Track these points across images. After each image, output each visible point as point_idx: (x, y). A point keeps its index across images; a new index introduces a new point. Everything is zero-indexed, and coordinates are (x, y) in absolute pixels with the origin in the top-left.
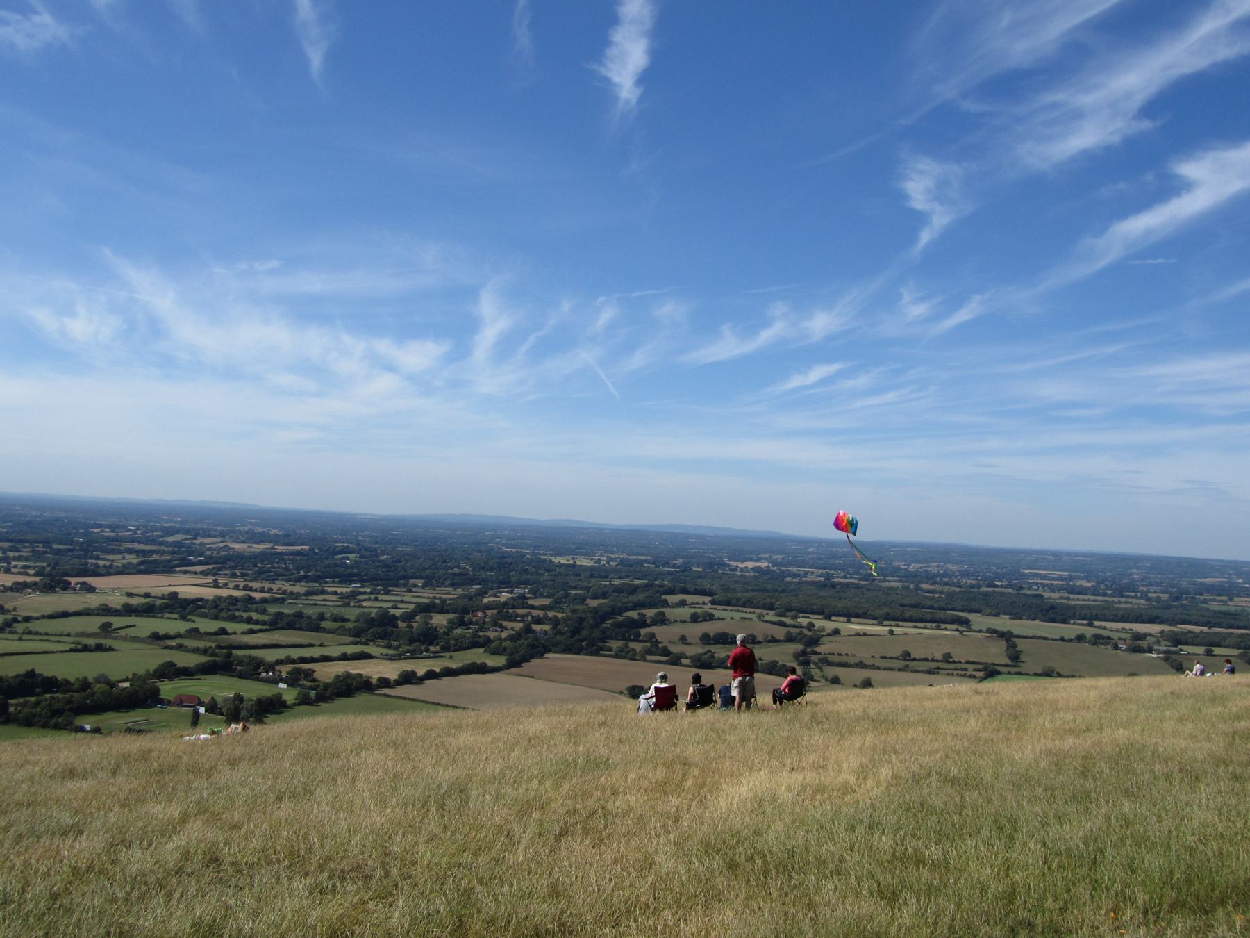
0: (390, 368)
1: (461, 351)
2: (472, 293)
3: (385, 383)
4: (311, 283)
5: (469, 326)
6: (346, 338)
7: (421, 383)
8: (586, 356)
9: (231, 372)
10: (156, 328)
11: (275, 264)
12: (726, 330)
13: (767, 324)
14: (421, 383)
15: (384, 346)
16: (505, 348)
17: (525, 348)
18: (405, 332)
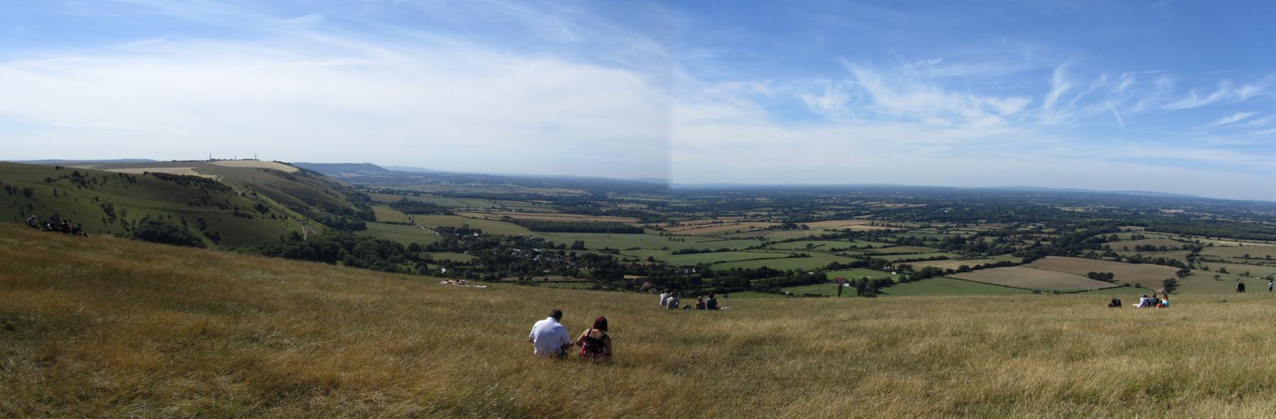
0: (994, 112)
1: (1038, 101)
2: (1050, 72)
3: (992, 120)
4: (958, 70)
5: (1048, 88)
6: (971, 97)
7: (1011, 120)
8: (1110, 105)
9: (906, 119)
10: (868, 98)
11: (939, 60)
14: (1011, 120)
15: (993, 101)
16: (1063, 101)
18: (1005, 94)
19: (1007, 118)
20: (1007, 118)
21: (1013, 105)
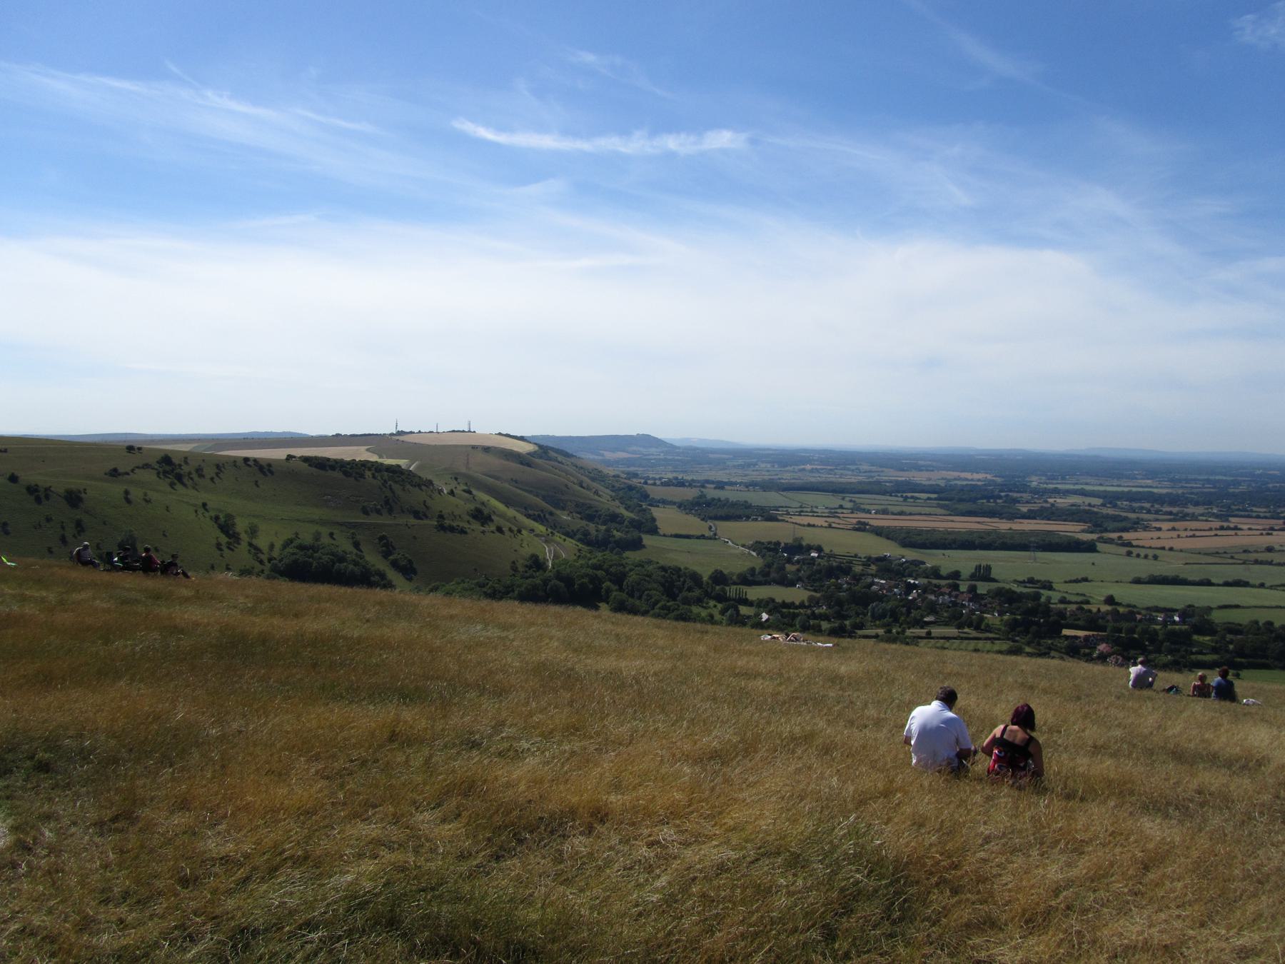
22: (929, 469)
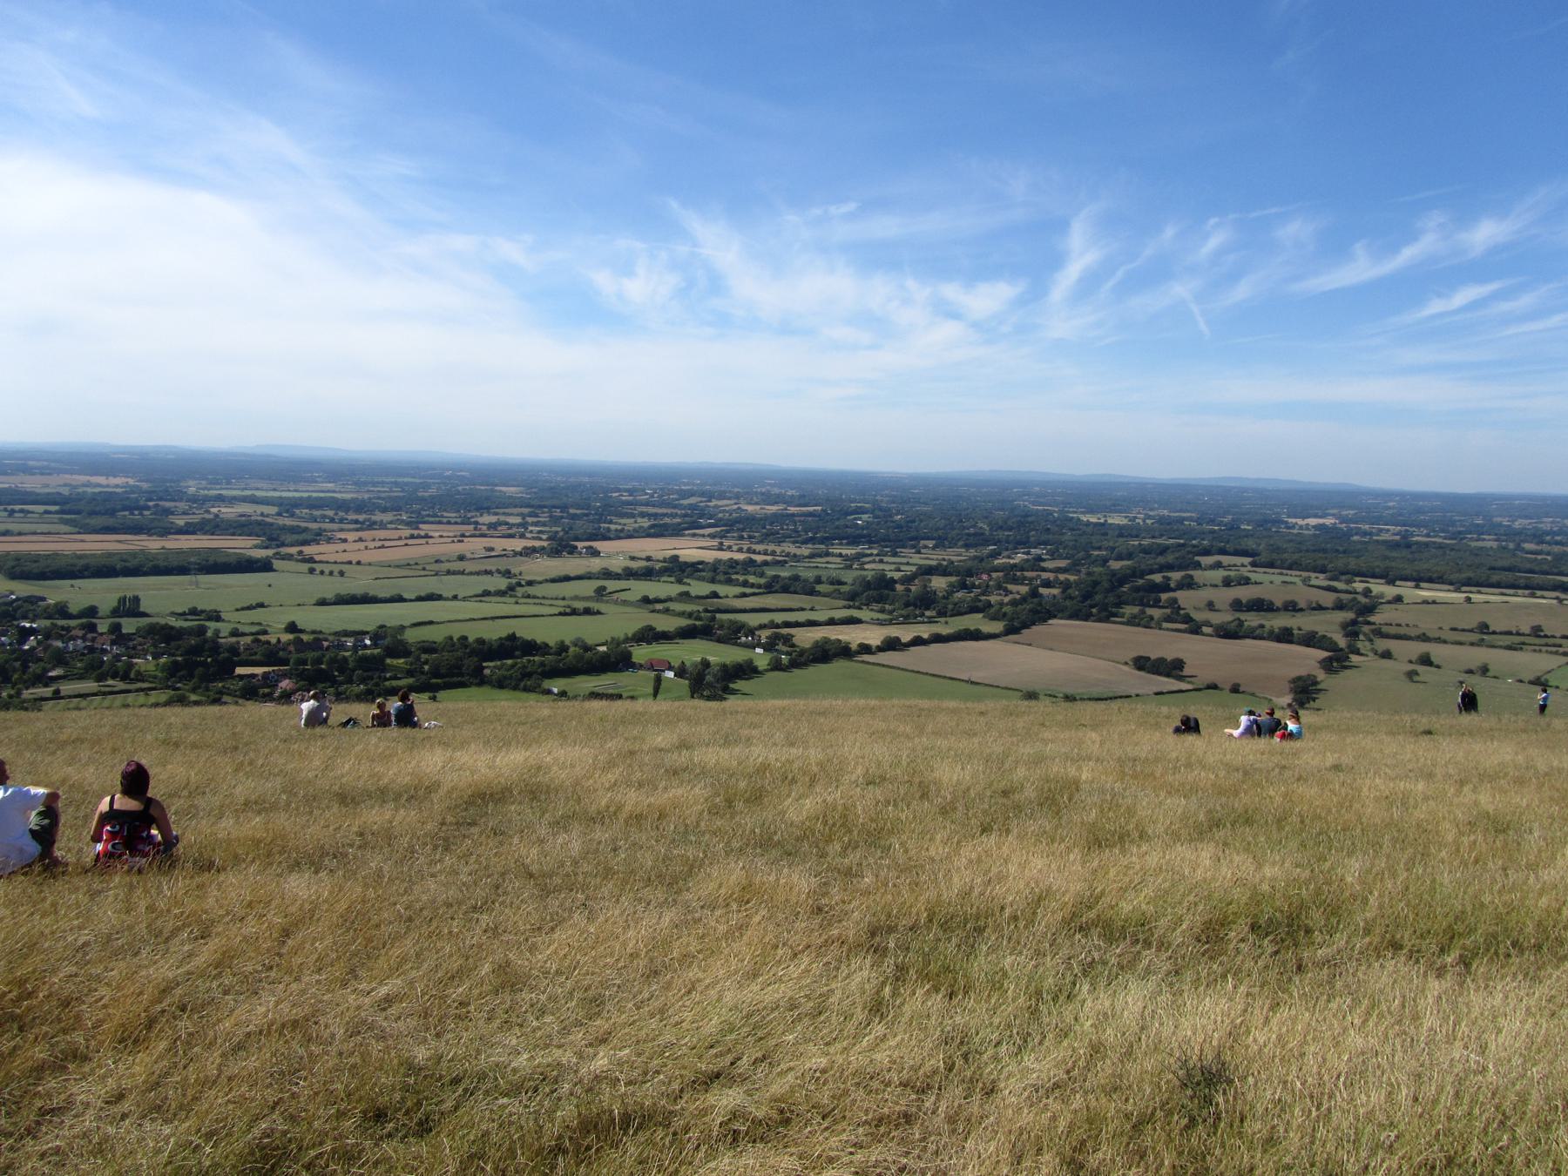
0: (953, 314)
1: (1037, 292)
2: (1062, 226)
3: (949, 330)
4: (885, 227)
5: (1056, 261)
6: (910, 283)
7: (985, 329)
8: (1181, 290)
9: (786, 328)
10: (717, 284)
11: (851, 207)
12: (1359, 249)
13: (1412, 236)
14: (985, 329)
15: (951, 291)
16: (1088, 285)
17: (1110, 284)
18: (976, 274)
19: (976, 325)
20: (976, 325)
21: (989, 298)
22: (44, 471)
